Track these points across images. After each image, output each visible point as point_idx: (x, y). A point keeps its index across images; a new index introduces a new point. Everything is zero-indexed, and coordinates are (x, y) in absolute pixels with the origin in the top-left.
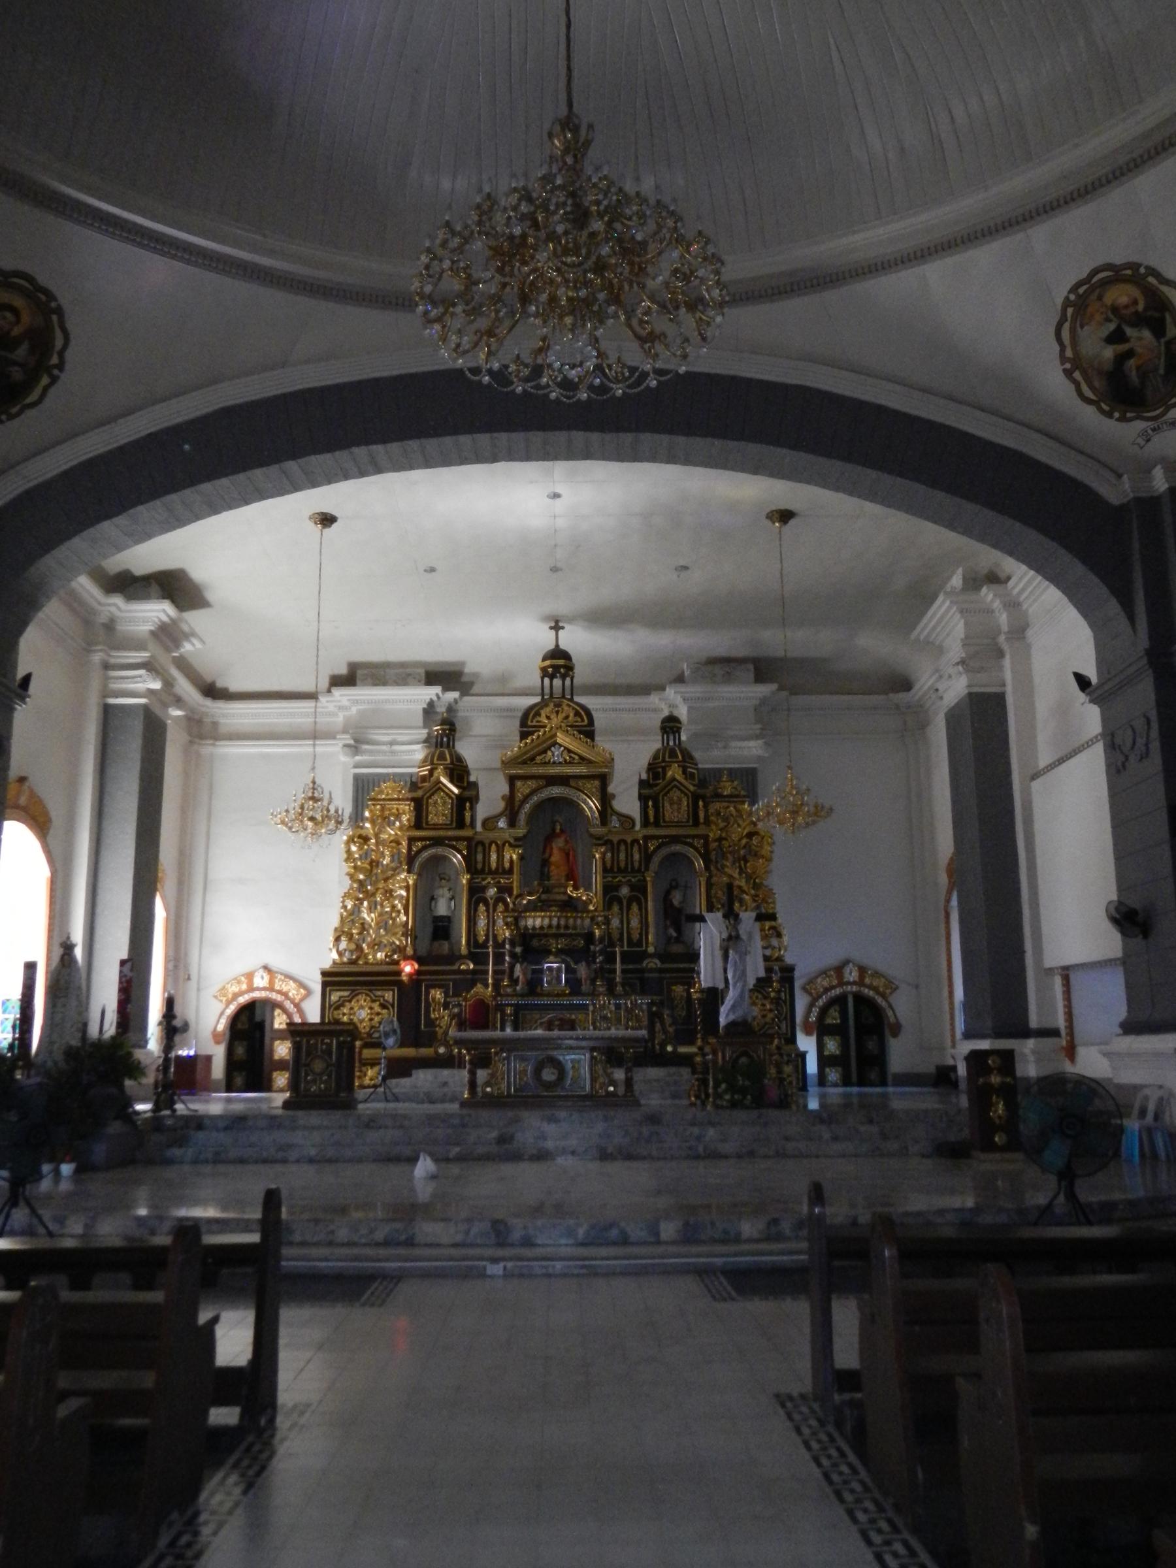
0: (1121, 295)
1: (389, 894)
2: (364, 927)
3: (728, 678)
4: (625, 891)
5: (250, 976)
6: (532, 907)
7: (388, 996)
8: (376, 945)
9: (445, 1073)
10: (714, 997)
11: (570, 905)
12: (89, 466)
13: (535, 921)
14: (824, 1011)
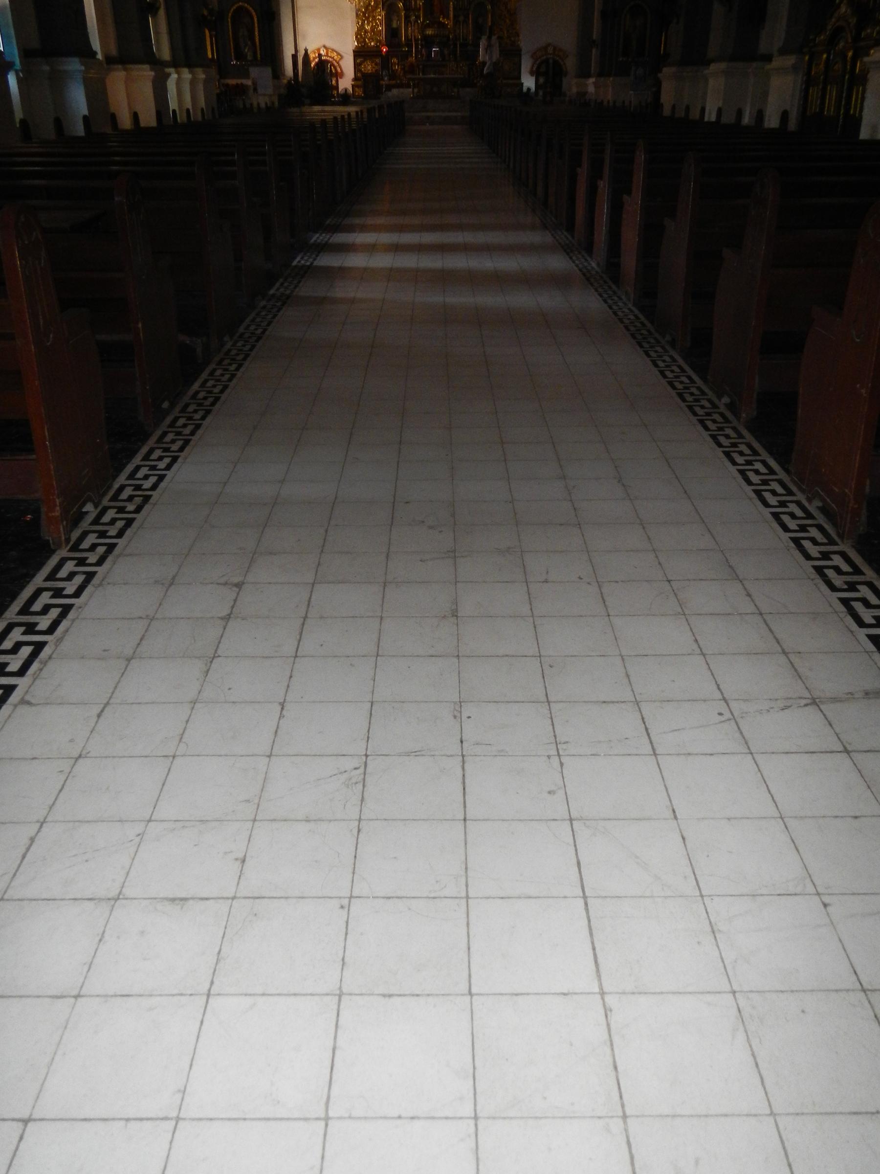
1: (374, 18)
2: (366, 32)
4: (461, 18)
5: (319, 50)
6: (428, 26)
7: (377, 60)
8: (371, 39)
9: (402, 90)
10: (484, 63)
11: (443, 25)
13: (429, 32)
14: (539, 67)
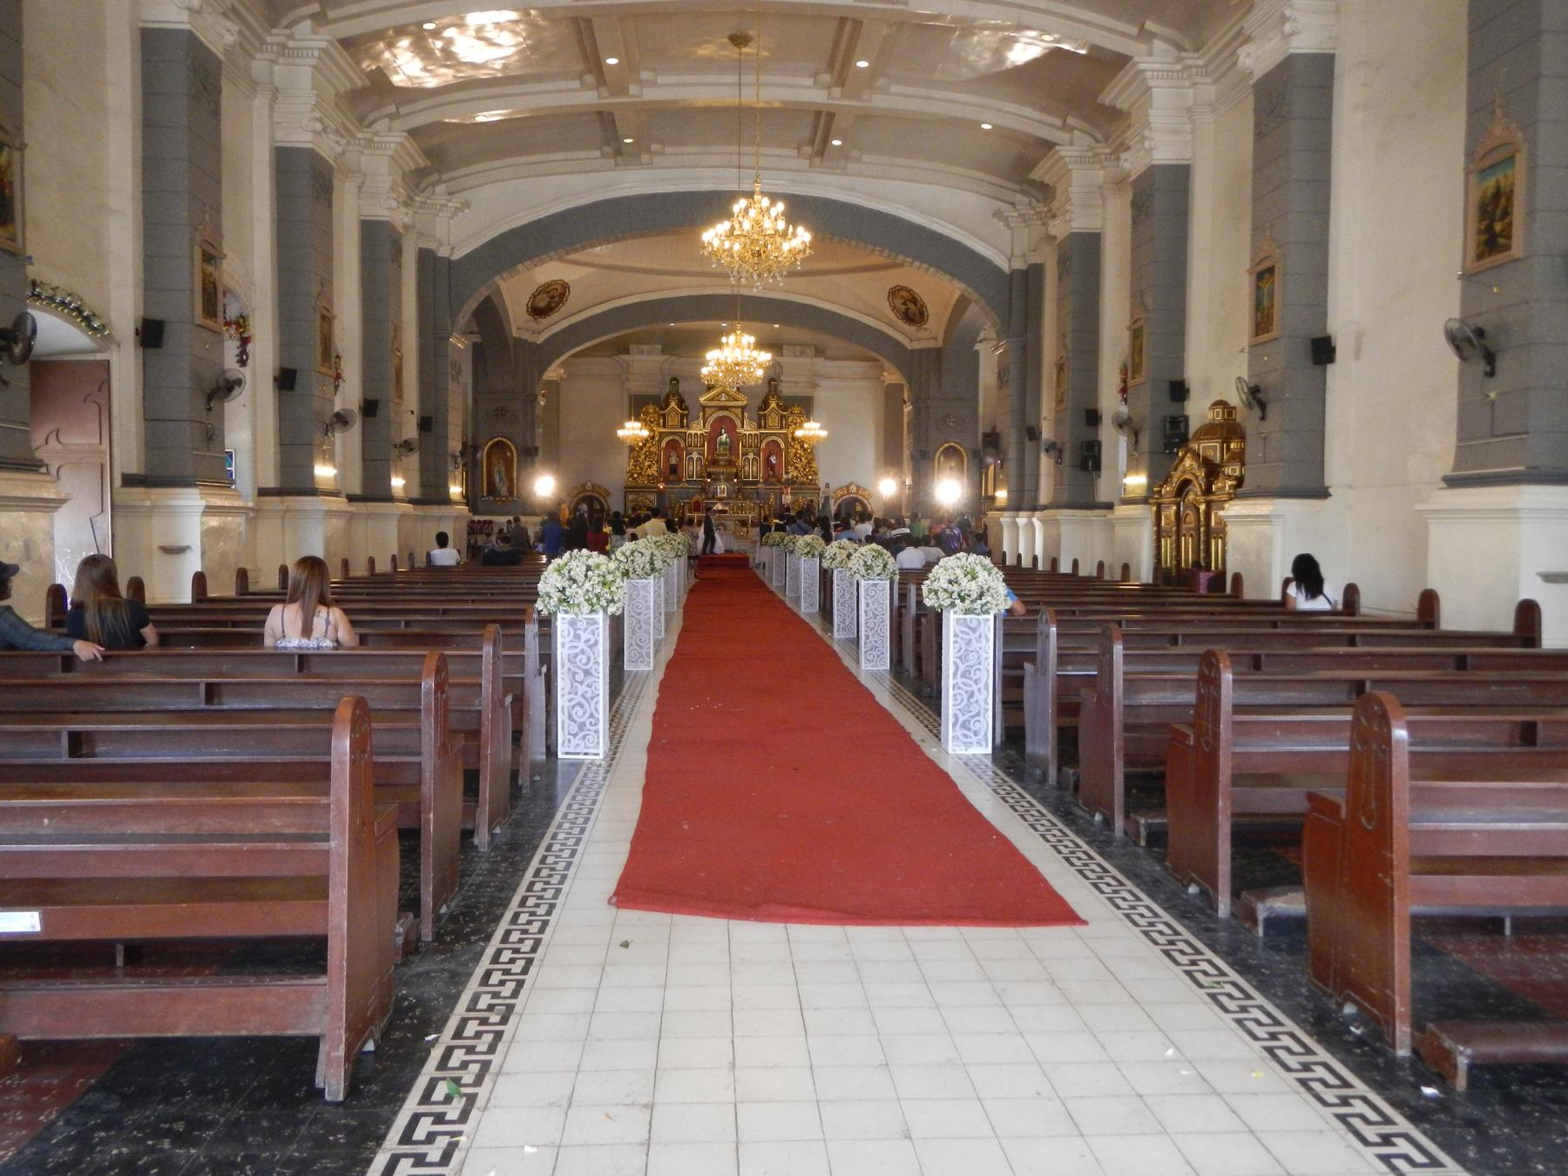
0: (905, 294)
3: (802, 354)
4: (751, 456)
12: (571, 326)
